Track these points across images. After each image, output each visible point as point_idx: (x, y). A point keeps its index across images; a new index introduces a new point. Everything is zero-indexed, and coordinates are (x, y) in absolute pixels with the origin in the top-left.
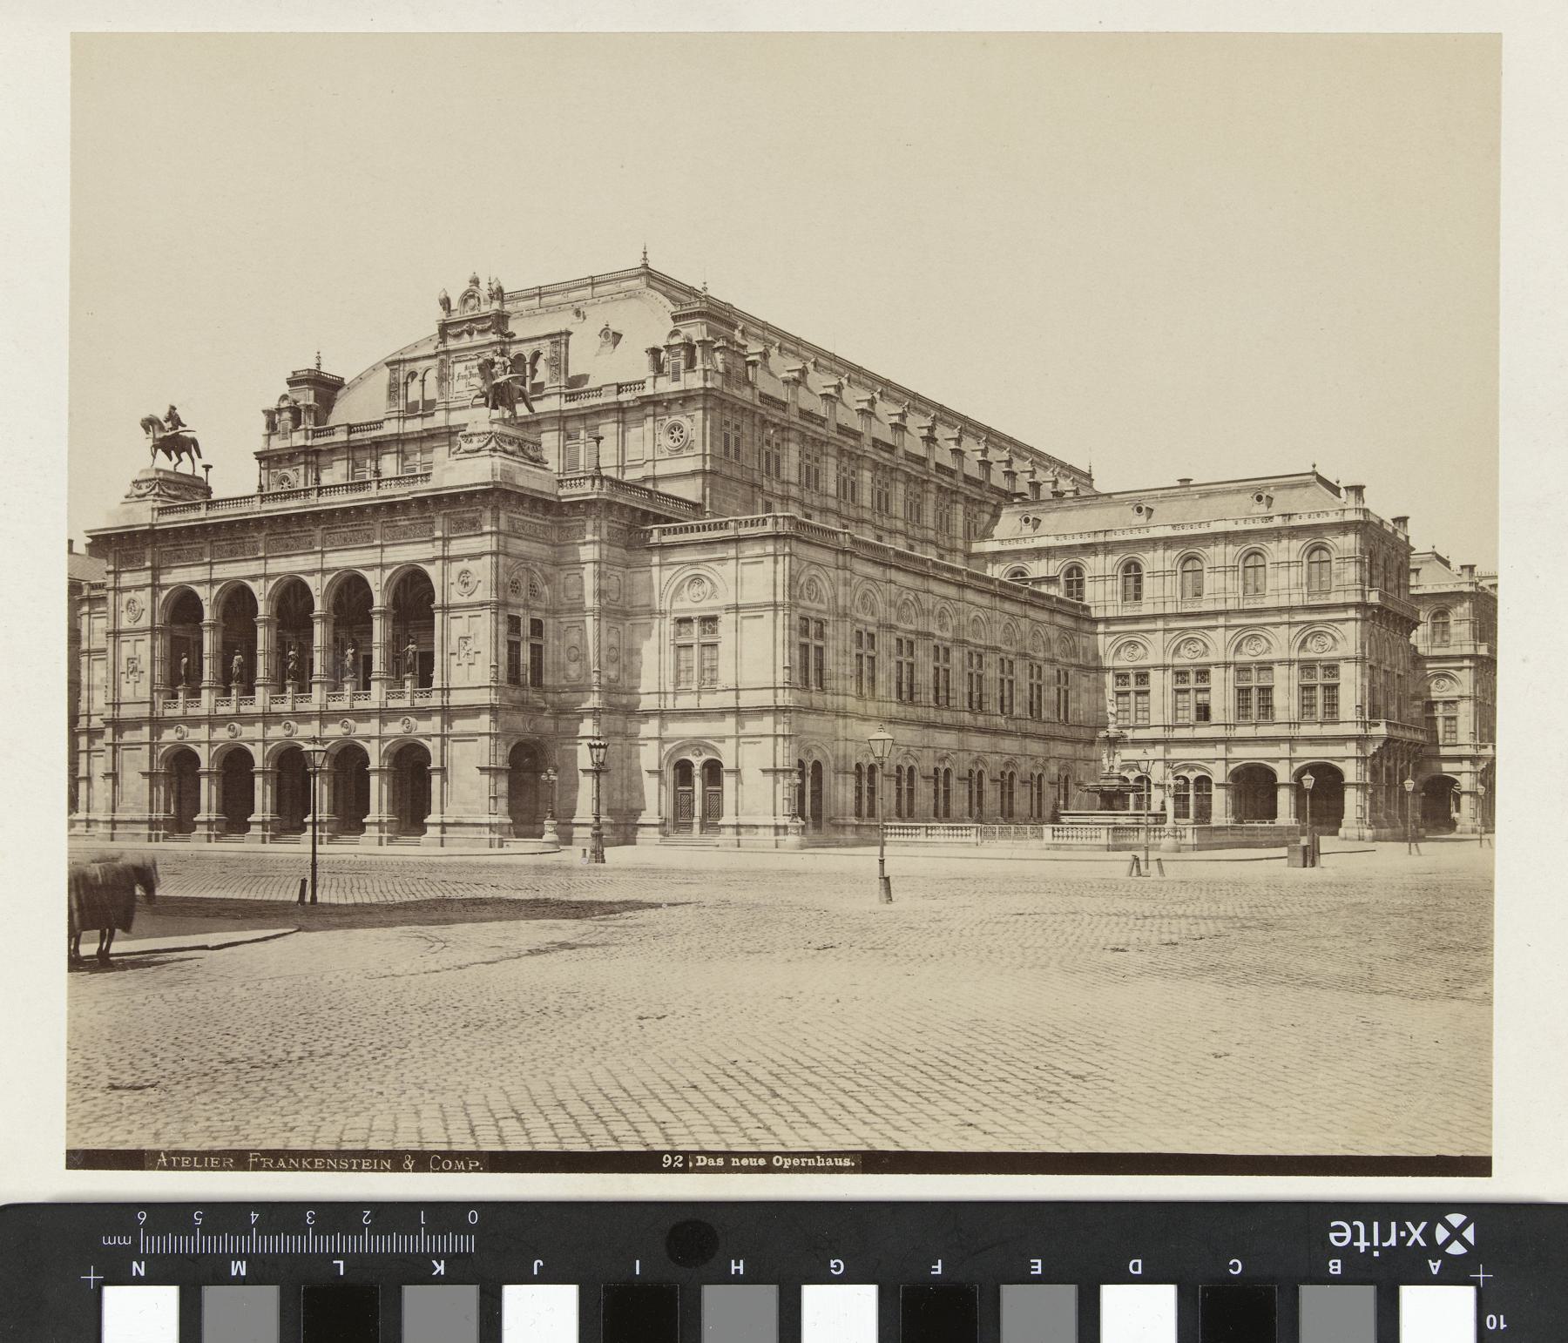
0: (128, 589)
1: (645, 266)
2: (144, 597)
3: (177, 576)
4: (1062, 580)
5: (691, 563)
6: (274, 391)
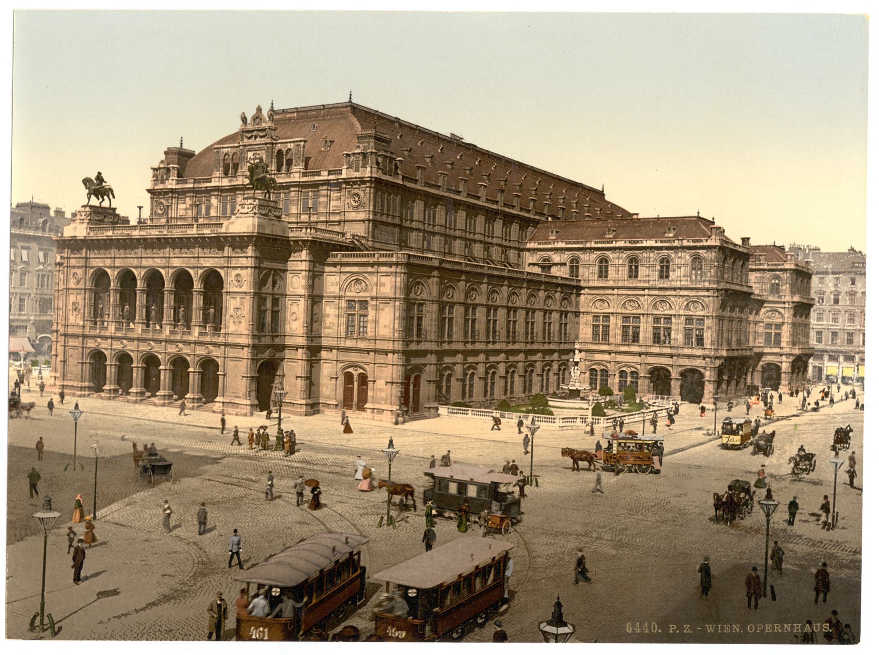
0: (74, 267)
1: (350, 101)
3: (98, 262)
5: (356, 273)
6: (157, 158)
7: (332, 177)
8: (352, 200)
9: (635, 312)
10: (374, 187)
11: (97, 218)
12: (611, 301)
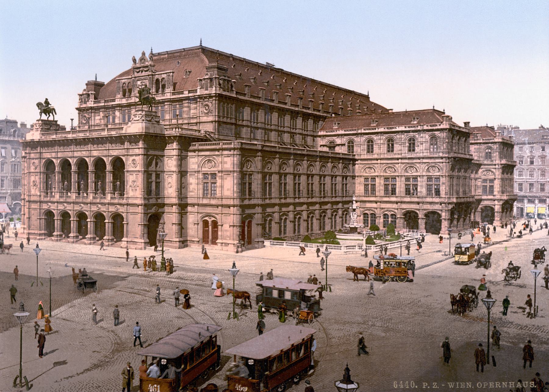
0: (33, 159)
1: (201, 45)
2: (37, 161)
3: (47, 155)
4: (346, 144)
5: (208, 156)
6: (81, 88)
7: (191, 95)
8: (204, 109)
9: (392, 174)
10: (218, 100)
11: (46, 128)
12: (376, 168)
